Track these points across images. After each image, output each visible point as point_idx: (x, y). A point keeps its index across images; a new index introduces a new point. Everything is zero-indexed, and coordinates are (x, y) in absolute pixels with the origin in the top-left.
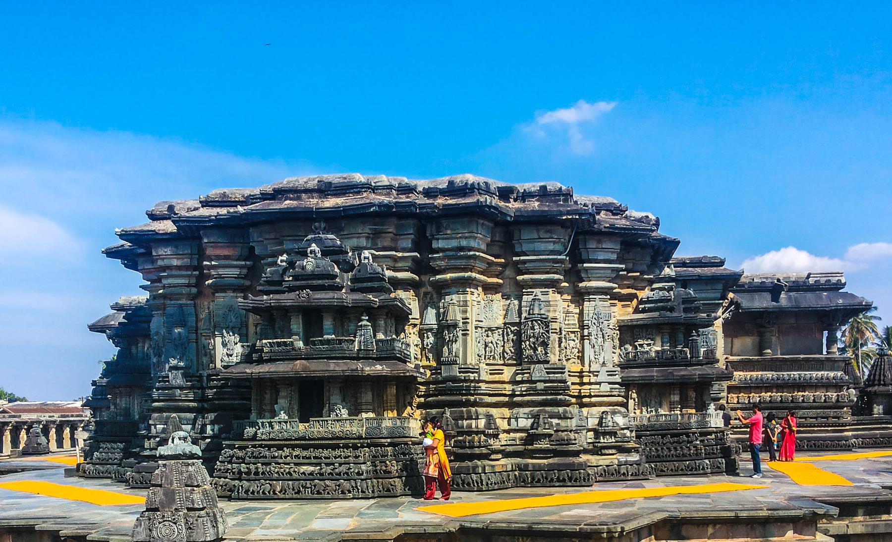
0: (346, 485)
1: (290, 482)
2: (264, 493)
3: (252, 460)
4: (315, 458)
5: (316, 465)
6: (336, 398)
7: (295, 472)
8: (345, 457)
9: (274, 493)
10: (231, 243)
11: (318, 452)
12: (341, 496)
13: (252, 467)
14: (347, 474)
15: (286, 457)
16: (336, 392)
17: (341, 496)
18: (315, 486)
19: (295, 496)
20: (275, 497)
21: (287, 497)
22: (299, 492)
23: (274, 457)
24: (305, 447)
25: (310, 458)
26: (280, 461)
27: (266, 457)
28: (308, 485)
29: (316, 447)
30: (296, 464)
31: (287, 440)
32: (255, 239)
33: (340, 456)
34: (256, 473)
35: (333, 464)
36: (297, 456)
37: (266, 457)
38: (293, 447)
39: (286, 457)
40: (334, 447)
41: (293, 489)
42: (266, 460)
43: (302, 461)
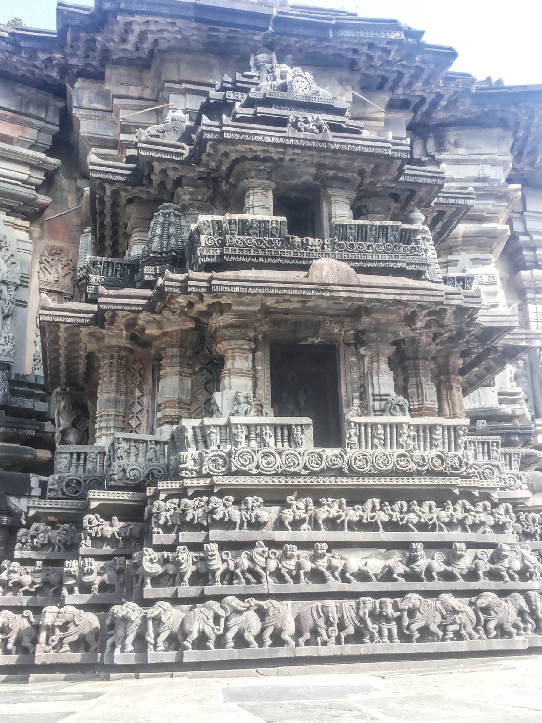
0: (507, 610)
1: (331, 604)
2: (241, 641)
3: (186, 536)
4: (391, 526)
5: (389, 546)
6: (384, 382)
7: (331, 568)
8: (475, 527)
9: (278, 640)
10: (18, 116)
11: (395, 511)
12: (498, 644)
13: (186, 557)
14: (494, 575)
15: (296, 524)
16: (384, 366)
17: (498, 644)
18: (412, 613)
19: (350, 649)
20: (282, 652)
21: (323, 651)
22: (358, 636)
23: (258, 525)
24: (356, 497)
25: (372, 526)
26: (280, 536)
27: (230, 524)
28: (390, 610)
29: (389, 496)
30: (333, 546)
31: (284, 474)
32: (85, 103)
33: (461, 523)
34: (202, 577)
35: (444, 546)
36: (333, 524)
37: (230, 524)
38: (317, 495)
39: (296, 524)
40: (442, 497)
41: (342, 627)
42: (235, 535)
43: (346, 536)
